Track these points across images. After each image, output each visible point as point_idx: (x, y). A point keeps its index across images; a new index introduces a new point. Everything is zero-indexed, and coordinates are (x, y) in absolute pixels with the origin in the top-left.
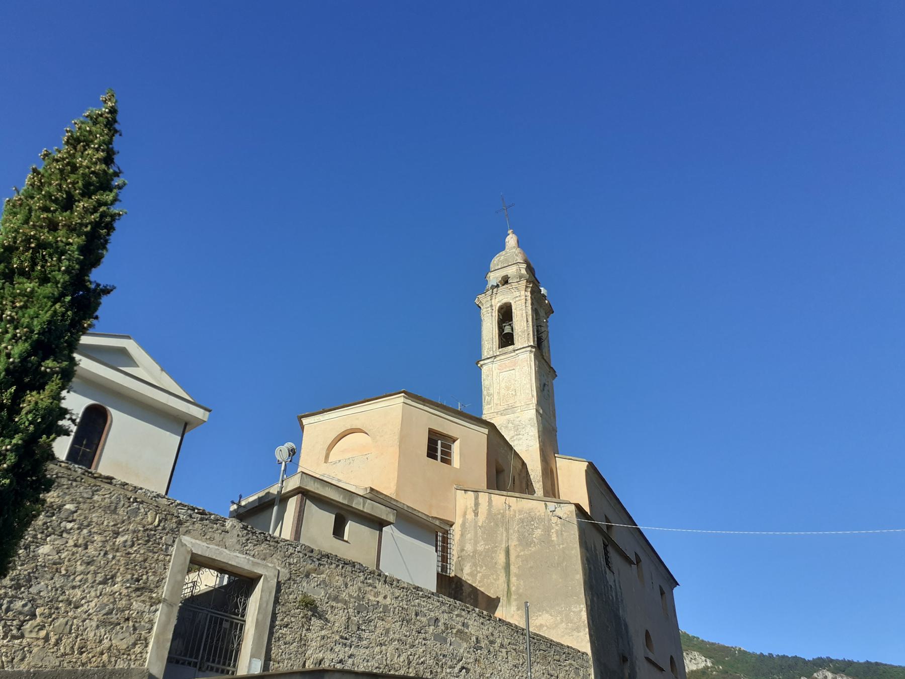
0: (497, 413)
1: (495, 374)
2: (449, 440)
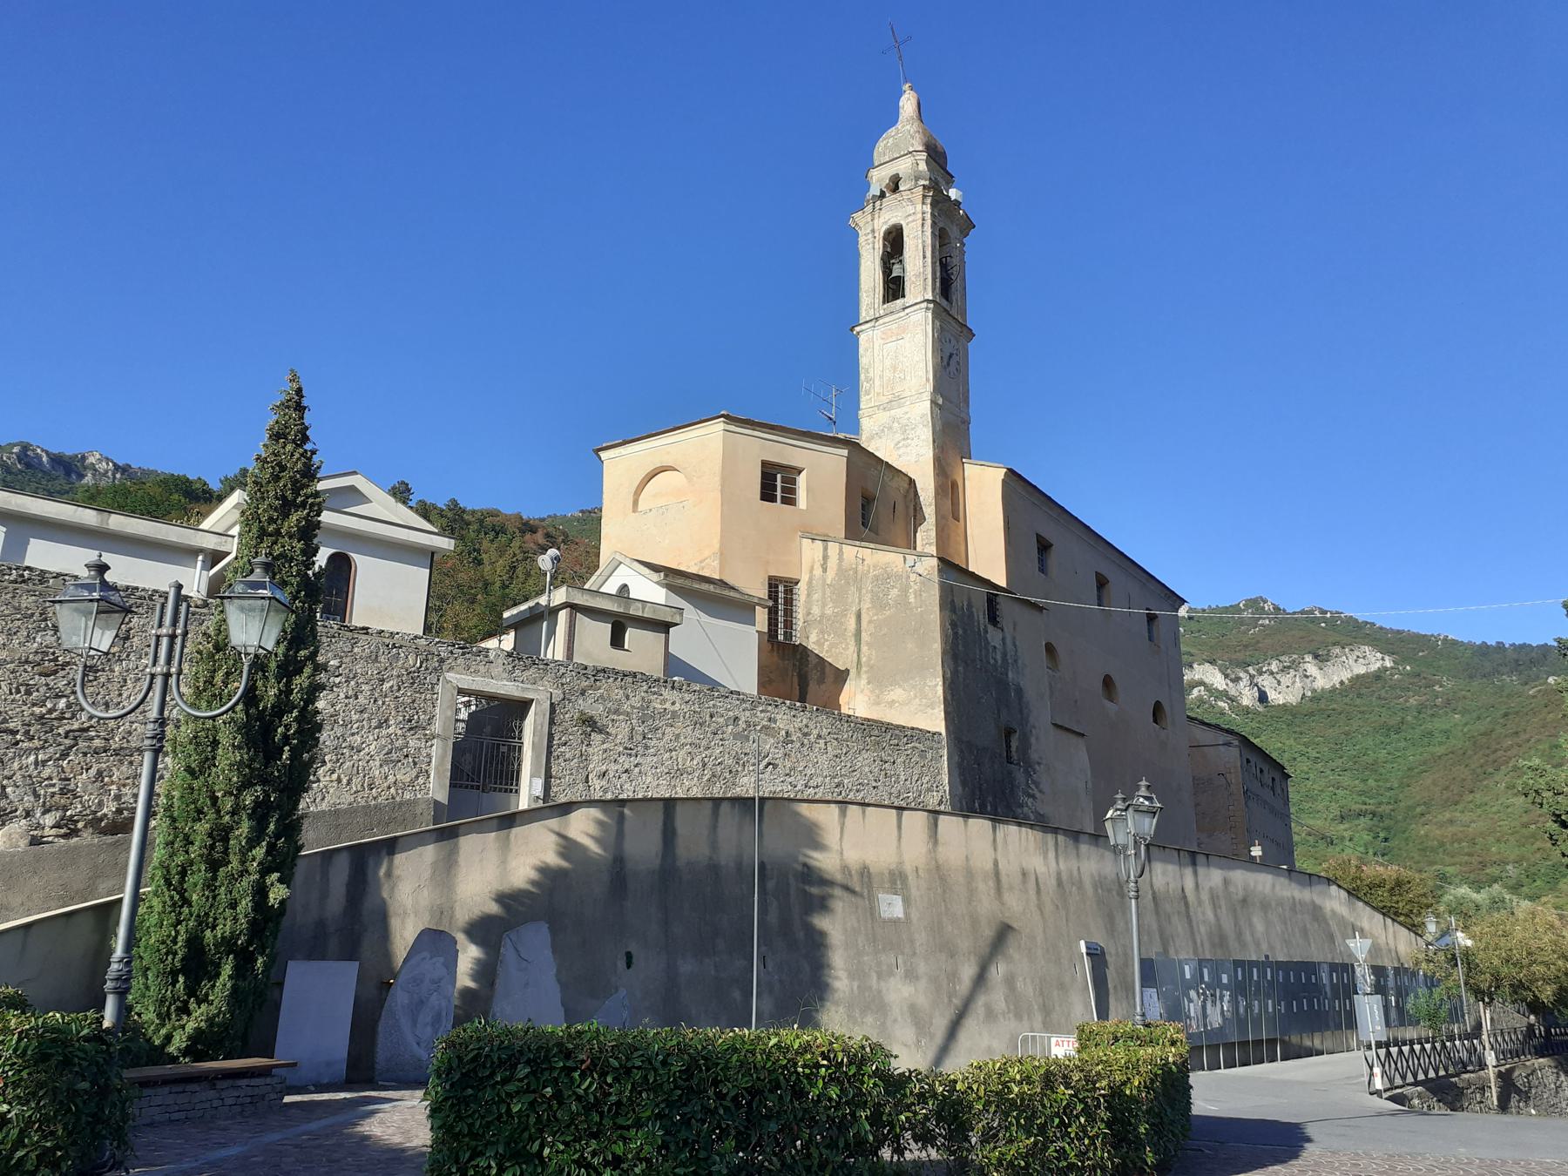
0: (878, 406)
1: (876, 347)
2: (791, 473)
